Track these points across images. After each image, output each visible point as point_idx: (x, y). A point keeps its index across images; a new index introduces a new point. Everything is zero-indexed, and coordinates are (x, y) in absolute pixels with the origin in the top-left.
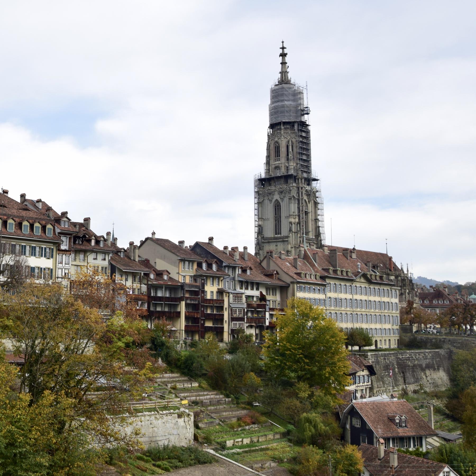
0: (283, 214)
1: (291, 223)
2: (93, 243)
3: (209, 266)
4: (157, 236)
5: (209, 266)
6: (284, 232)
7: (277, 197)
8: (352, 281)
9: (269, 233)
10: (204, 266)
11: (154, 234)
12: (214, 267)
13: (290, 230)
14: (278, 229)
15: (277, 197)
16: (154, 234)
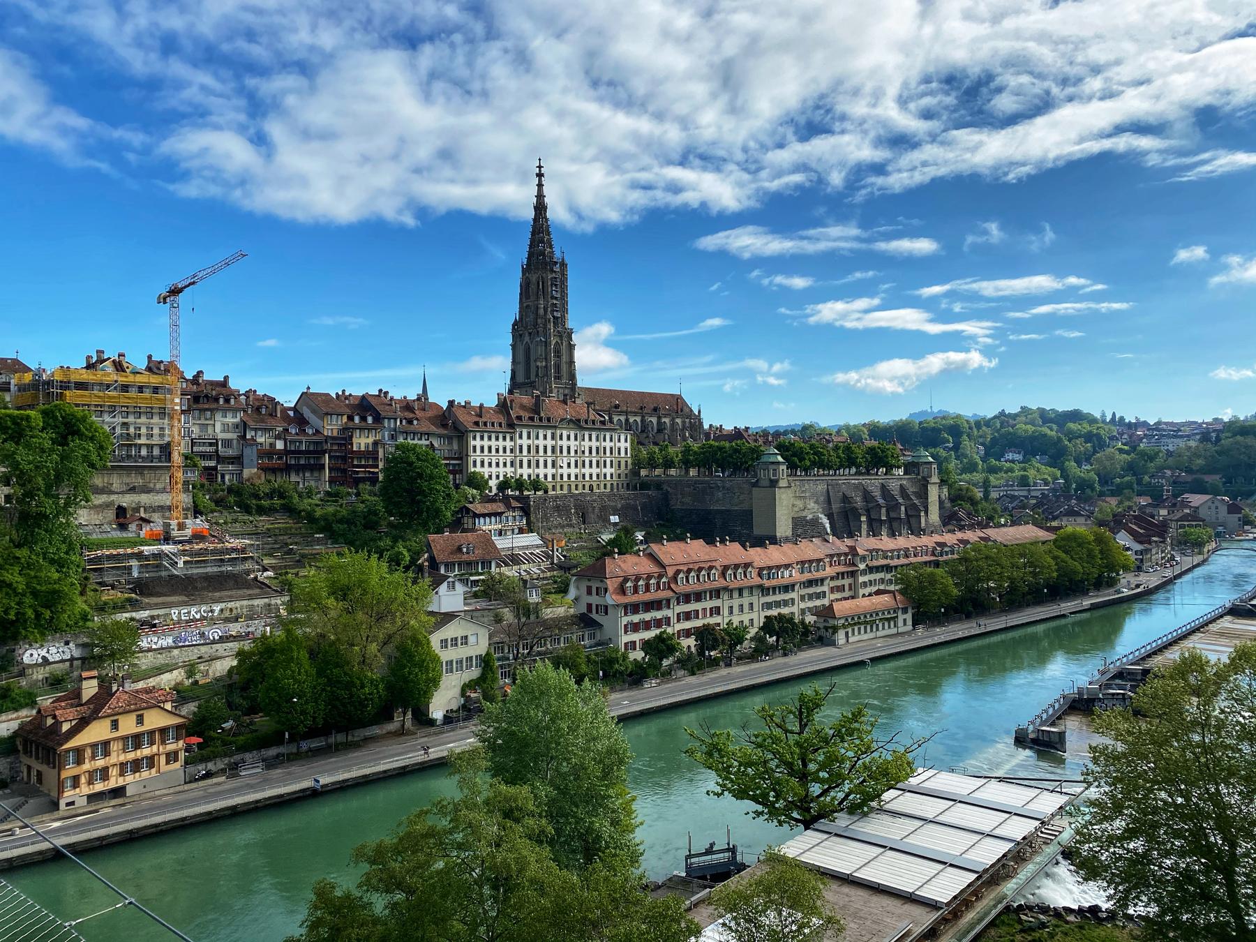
0: (532, 359)
1: (537, 367)
2: (221, 401)
3: (364, 419)
4: (311, 391)
5: (364, 419)
6: (533, 378)
7: (527, 339)
8: (555, 427)
9: (521, 378)
10: (357, 419)
11: (309, 388)
12: (370, 420)
13: (537, 375)
14: (528, 376)
15: (527, 339)
16: (309, 388)
